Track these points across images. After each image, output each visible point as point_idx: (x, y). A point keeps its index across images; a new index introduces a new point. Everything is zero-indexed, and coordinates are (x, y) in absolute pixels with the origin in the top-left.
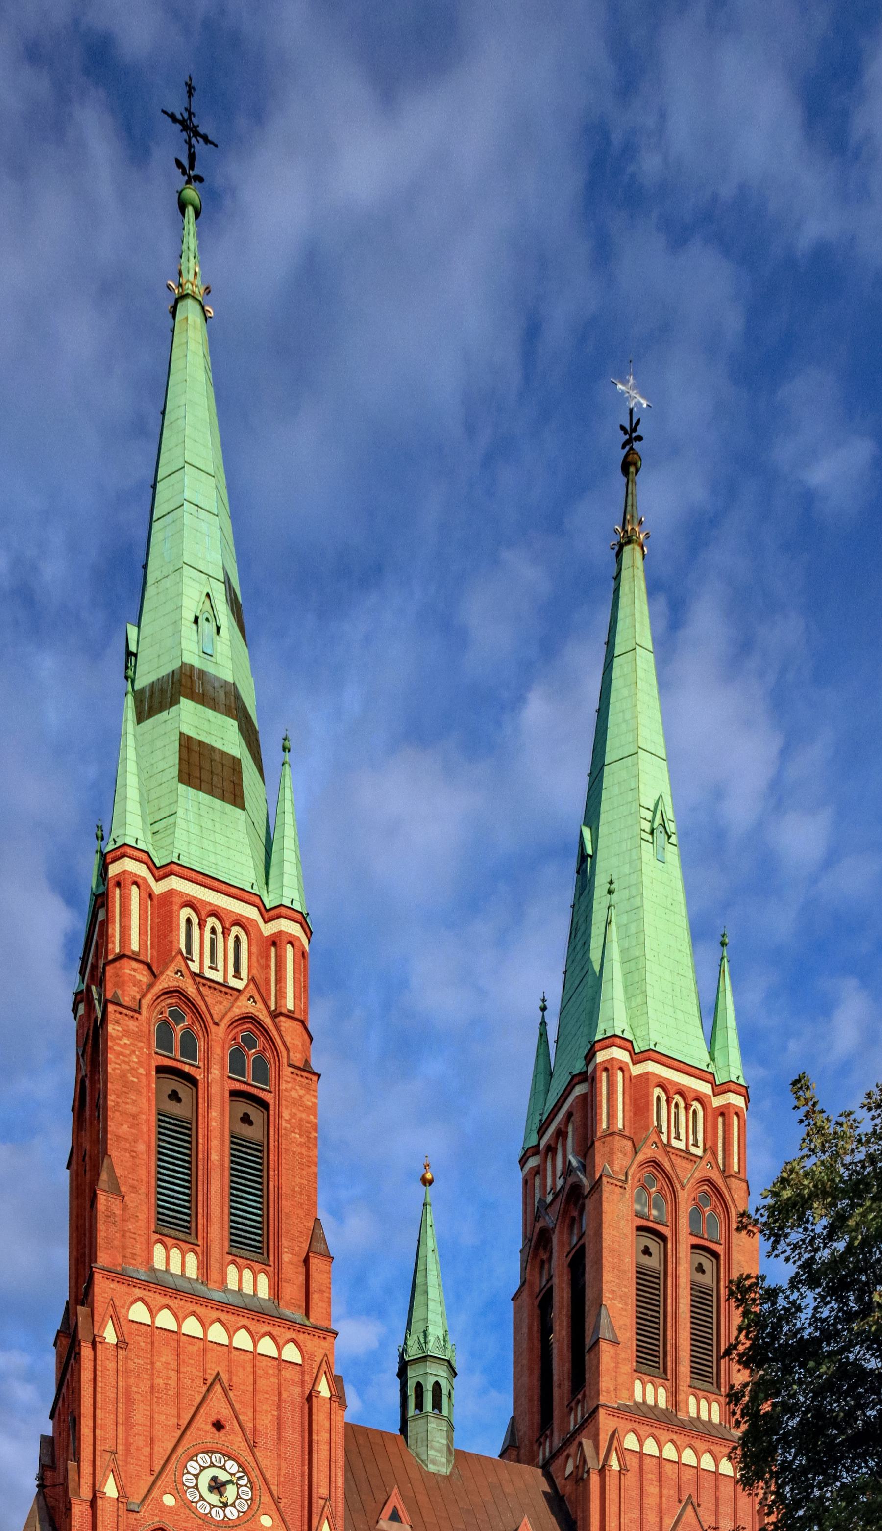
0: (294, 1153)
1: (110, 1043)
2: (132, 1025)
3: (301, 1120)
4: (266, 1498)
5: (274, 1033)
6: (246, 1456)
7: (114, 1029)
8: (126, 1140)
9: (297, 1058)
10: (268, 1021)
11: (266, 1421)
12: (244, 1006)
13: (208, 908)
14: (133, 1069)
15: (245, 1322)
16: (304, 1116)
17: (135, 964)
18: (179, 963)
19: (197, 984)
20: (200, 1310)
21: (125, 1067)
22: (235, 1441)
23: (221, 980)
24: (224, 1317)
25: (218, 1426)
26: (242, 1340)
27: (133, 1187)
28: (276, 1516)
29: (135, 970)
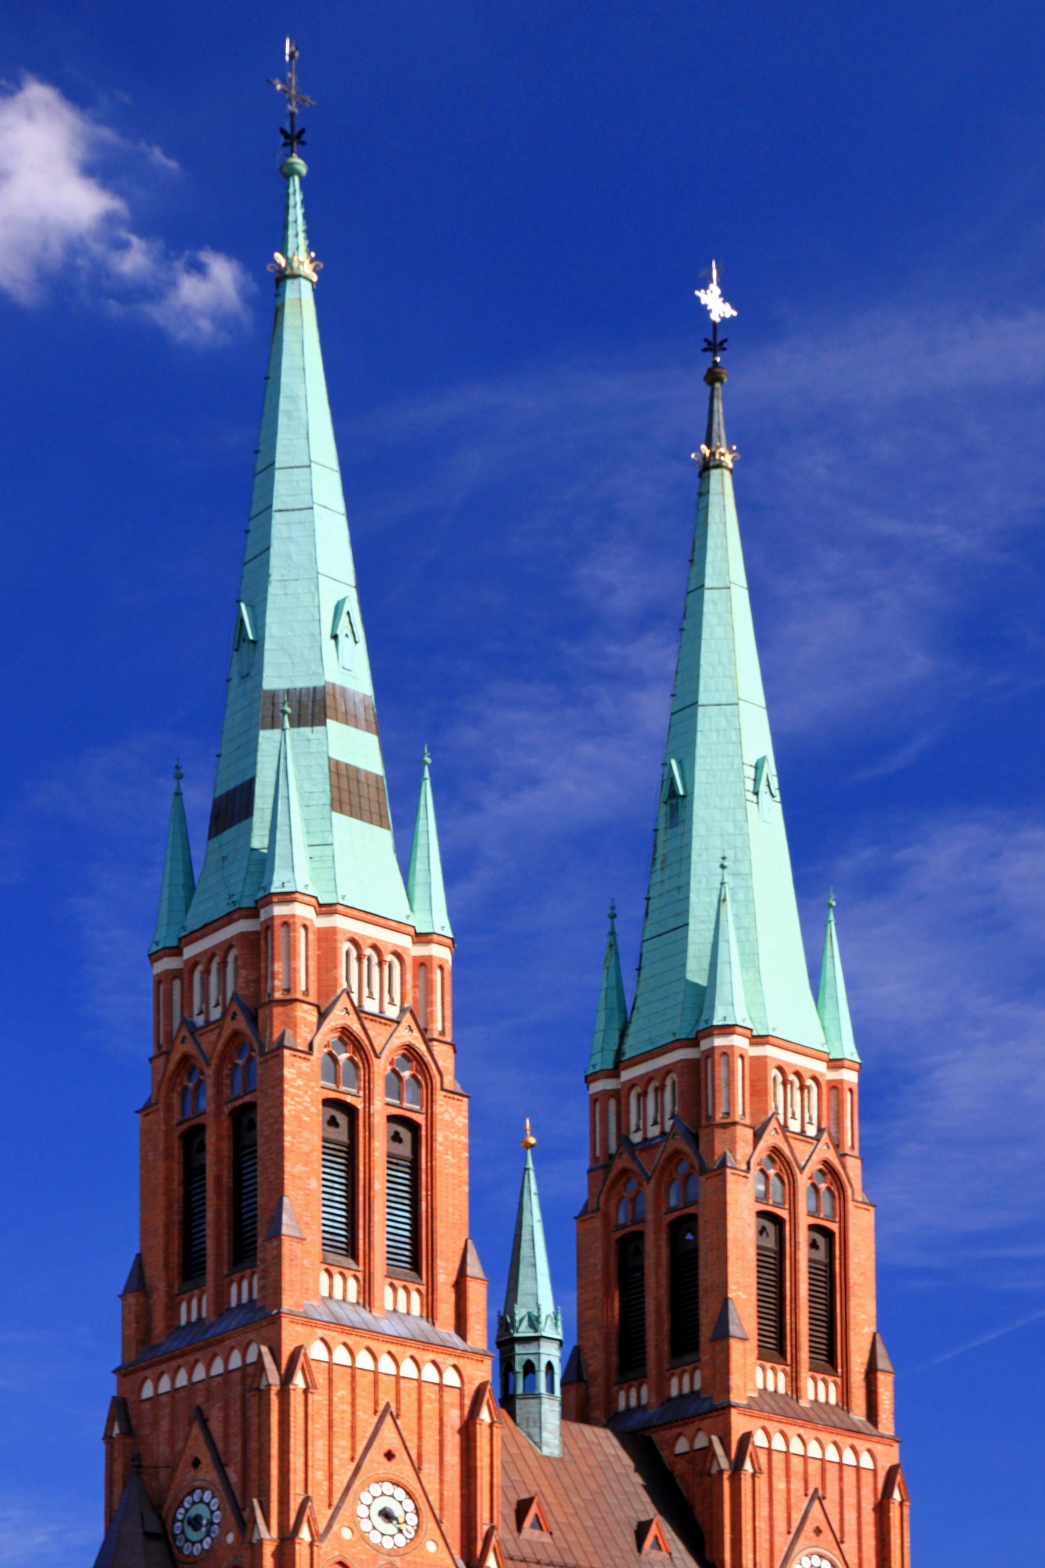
0: (447, 1174)
1: (286, 1086)
2: (305, 1066)
3: (453, 1141)
5: (428, 1058)
7: (289, 1072)
8: (300, 1178)
14: (307, 1108)
16: (456, 1137)
17: (306, 1007)
18: (344, 1001)
19: (360, 1019)
21: (299, 1107)
22: (402, 1468)
27: (307, 1224)
29: (306, 1012)
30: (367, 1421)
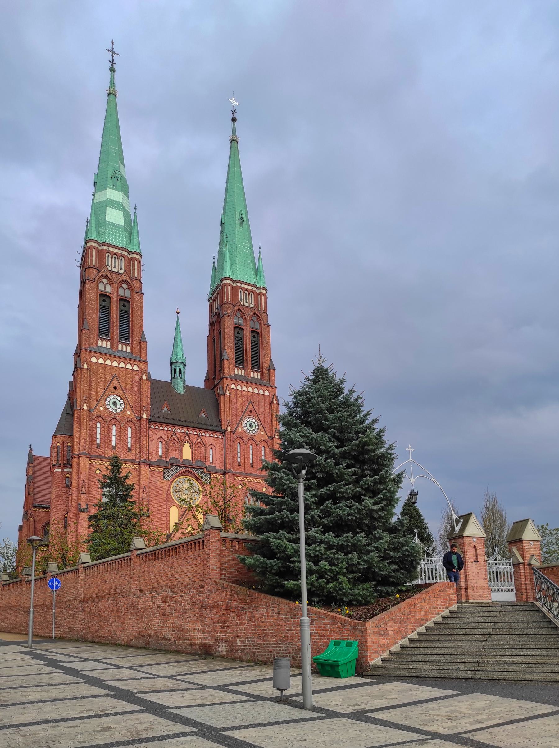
4: (128, 407)
6: (123, 395)
10: (130, 281)
11: (129, 386)
12: (123, 278)
13: (114, 253)
15: (123, 360)
20: (111, 358)
22: (120, 392)
23: (117, 271)
24: (117, 359)
25: (115, 388)
26: (122, 365)
28: (131, 411)
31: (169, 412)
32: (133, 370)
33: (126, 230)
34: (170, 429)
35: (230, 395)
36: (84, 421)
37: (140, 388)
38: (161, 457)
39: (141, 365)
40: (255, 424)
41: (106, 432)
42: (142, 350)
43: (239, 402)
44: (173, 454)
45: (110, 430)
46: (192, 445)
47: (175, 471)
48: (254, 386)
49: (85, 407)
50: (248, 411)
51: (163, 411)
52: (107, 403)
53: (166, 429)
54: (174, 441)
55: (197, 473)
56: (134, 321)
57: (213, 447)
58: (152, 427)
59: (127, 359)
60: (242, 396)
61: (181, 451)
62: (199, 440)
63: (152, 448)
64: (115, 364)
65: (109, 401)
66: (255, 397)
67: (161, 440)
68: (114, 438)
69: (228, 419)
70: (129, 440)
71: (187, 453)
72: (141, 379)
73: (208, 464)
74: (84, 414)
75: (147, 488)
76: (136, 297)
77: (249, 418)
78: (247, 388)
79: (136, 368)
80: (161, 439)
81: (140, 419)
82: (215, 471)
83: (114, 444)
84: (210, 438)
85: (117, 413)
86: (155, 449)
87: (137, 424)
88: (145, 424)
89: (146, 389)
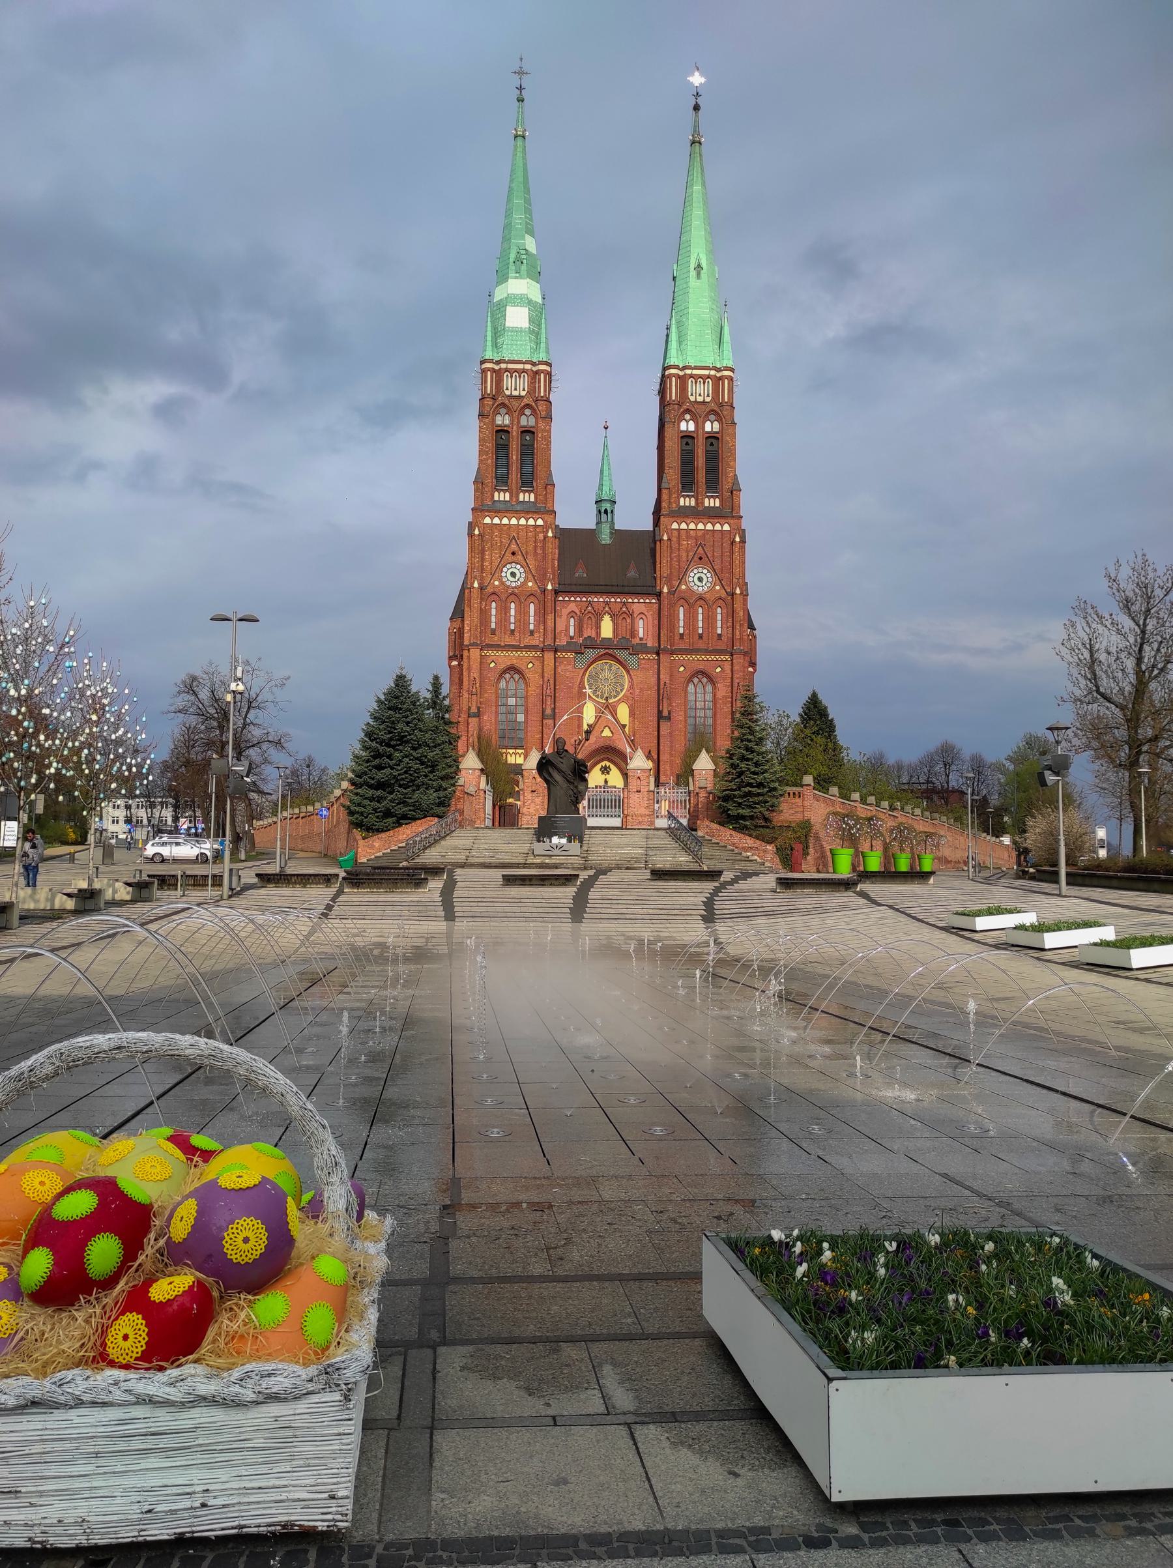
9: (543, 414)
11: (531, 548)
22: (520, 558)
30: (505, 541)
31: (585, 575)
32: (536, 526)
33: (531, 331)
34: (584, 599)
35: (669, 539)
36: (476, 603)
37: (544, 548)
38: (572, 638)
39: (549, 518)
40: (706, 574)
41: (504, 611)
42: (549, 496)
43: (683, 547)
44: (589, 632)
45: (507, 610)
46: (614, 617)
47: (590, 654)
48: (705, 521)
49: (476, 585)
50: (696, 558)
51: (577, 575)
52: (503, 574)
53: (578, 599)
54: (590, 615)
55: (621, 654)
56: (539, 458)
57: (642, 616)
58: (561, 598)
59: (528, 512)
60: (688, 537)
61: (598, 627)
62: (624, 609)
63: (560, 627)
64: (514, 521)
65: (506, 572)
66: (707, 536)
67: (573, 614)
68: (512, 620)
69: (665, 575)
70: (532, 620)
71: (607, 629)
72: (546, 537)
73: (636, 641)
74: (475, 594)
75: (552, 682)
76: (542, 425)
77: (697, 568)
78: (696, 525)
79: (540, 522)
80: (572, 614)
81: (544, 591)
82: (644, 650)
83: (512, 627)
84: (639, 604)
85: (515, 587)
86: (564, 629)
87: (541, 597)
88: (550, 597)
89: (553, 550)
